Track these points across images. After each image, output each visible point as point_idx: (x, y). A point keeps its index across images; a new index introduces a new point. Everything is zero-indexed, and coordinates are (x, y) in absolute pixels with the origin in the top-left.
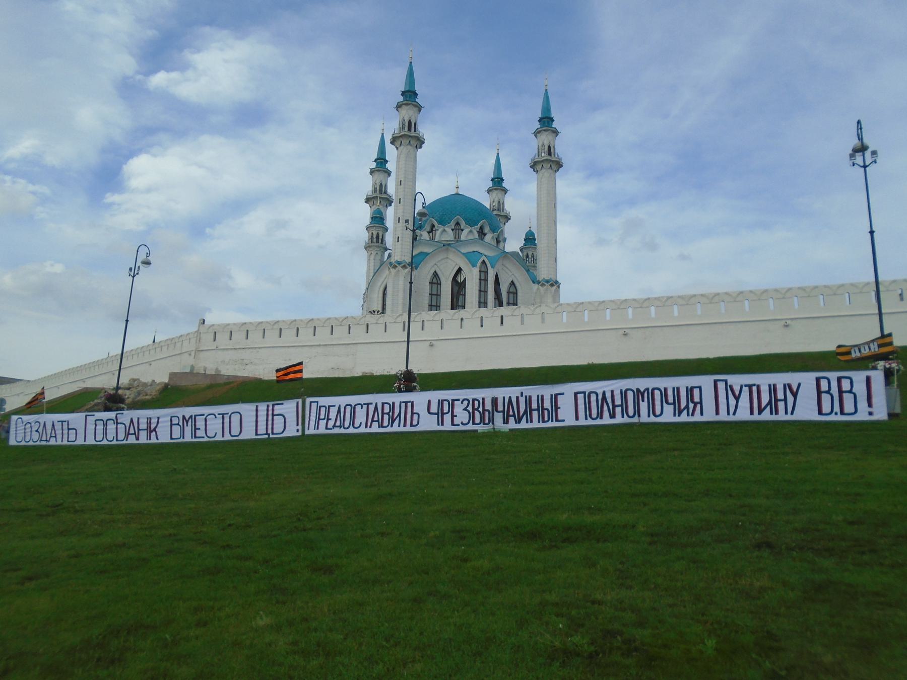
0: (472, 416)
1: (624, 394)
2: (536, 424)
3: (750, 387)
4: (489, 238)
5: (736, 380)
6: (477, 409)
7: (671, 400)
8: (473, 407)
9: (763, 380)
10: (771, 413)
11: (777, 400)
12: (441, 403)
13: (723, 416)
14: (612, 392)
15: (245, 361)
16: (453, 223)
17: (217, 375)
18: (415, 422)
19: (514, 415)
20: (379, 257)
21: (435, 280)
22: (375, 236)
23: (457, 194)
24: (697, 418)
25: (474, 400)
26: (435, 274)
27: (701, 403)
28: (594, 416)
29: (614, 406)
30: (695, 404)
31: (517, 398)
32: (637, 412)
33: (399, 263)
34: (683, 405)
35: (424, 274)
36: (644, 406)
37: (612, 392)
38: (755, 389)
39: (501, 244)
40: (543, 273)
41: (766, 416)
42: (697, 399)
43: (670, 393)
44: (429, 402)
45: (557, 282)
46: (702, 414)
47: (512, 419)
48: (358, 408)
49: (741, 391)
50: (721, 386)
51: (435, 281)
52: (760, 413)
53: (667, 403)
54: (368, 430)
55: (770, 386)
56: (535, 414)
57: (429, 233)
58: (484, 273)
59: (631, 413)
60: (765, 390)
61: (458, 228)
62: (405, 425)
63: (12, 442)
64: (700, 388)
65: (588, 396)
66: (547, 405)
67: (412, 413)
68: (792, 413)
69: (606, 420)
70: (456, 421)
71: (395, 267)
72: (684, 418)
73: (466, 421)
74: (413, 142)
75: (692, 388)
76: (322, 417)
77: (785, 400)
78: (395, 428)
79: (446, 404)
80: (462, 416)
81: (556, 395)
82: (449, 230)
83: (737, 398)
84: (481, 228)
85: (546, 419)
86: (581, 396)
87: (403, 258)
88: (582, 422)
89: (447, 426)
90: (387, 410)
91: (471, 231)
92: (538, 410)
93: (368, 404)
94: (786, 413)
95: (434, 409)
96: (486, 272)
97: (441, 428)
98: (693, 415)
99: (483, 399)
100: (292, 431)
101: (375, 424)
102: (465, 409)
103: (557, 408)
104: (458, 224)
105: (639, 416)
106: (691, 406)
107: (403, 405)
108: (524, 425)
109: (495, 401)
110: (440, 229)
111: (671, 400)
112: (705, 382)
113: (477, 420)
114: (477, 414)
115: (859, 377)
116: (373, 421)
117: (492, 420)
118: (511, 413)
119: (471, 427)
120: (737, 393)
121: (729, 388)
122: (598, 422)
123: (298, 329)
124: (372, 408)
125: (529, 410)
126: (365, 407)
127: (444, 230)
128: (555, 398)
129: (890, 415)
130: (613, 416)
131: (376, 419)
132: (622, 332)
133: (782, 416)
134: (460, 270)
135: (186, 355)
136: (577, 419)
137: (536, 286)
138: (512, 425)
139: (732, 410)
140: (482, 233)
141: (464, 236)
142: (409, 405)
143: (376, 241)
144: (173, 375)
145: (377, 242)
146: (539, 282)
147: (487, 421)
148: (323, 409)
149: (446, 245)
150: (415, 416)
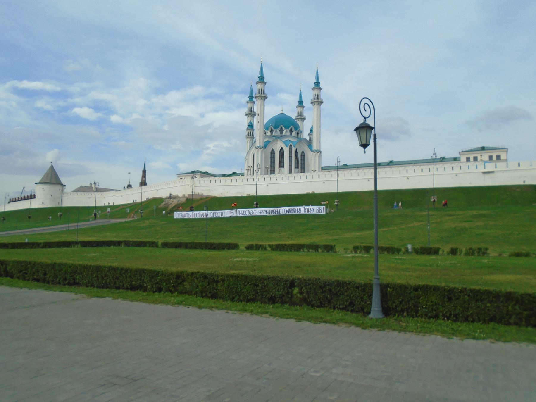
4: (294, 133)
16: (279, 128)
17: (202, 195)
21: (273, 152)
23: (282, 114)
39: (300, 135)
40: (315, 148)
45: (320, 151)
58: (291, 149)
61: (281, 131)
63: (175, 217)
74: (263, 98)
80: (265, 213)
84: (291, 129)
96: (292, 149)
100: (235, 215)
104: (282, 128)
110: (275, 130)
115: (322, 207)
129: (327, 213)
134: (282, 148)
135: (187, 186)
140: (291, 131)
141: (284, 133)
143: (251, 136)
149: (277, 138)
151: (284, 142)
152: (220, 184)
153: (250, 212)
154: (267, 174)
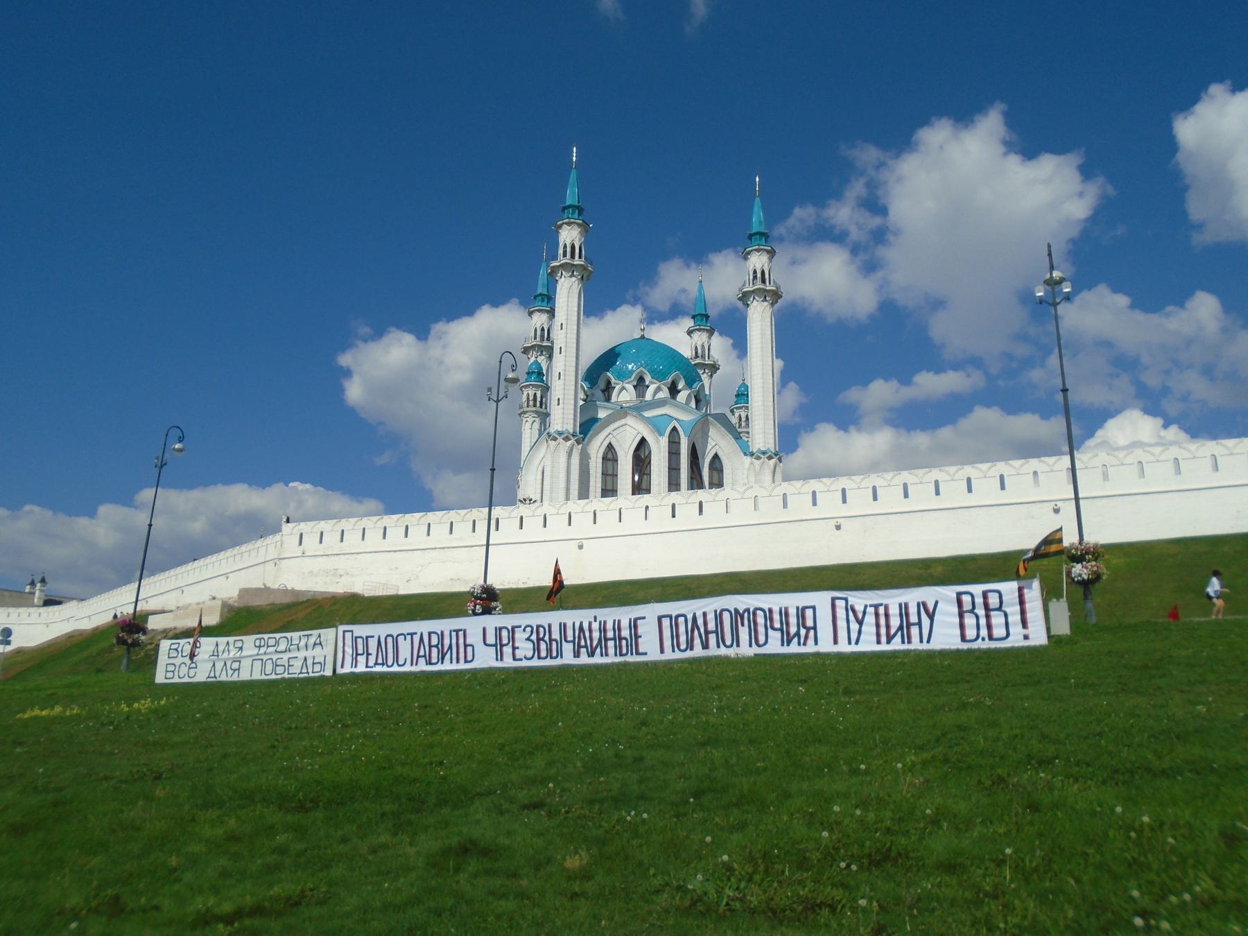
0: (537, 649)
1: (719, 617)
2: (611, 659)
3: (876, 607)
5: (859, 600)
6: (543, 639)
7: (777, 625)
8: (539, 637)
9: (893, 599)
10: (903, 642)
11: (909, 625)
12: (499, 630)
13: (844, 647)
14: (705, 614)
15: (340, 572)
18: (469, 658)
19: (586, 646)
20: (536, 426)
21: (610, 456)
24: (810, 648)
25: (538, 627)
26: (610, 447)
27: (815, 628)
28: (683, 646)
29: (707, 632)
30: (808, 629)
31: (590, 624)
32: (736, 640)
33: (560, 434)
34: (793, 630)
35: (596, 448)
36: (744, 633)
37: (705, 614)
38: (882, 610)
41: (897, 645)
42: (810, 623)
43: (776, 617)
44: (484, 629)
46: (816, 643)
47: (583, 650)
48: (401, 638)
49: (864, 613)
50: (840, 604)
51: (610, 456)
52: (888, 642)
53: (773, 628)
54: (414, 669)
55: (900, 605)
56: (611, 644)
57: (603, 391)
59: (728, 642)
60: (894, 610)
61: (640, 384)
62: (458, 661)
64: (814, 608)
65: (674, 620)
66: (625, 633)
67: (466, 646)
68: (928, 641)
69: (698, 652)
70: (519, 653)
71: (555, 439)
72: (794, 648)
73: (530, 654)
75: (804, 608)
76: (360, 651)
77: (919, 624)
78: (447, 666)
79: (505, 633)
80: (525, 648)
81: (636, 620)
82: (630, 387)
83: (860, 623)
85: (624, 651)
86: (666, 622)
87: (565, 427)
88: (669, 655)
89: (508, 662)
90: (435, 641)
91: (658, 389)
92: (614, 639)
93: (412, 634)
94: (921, 641)
95: (491, 639)
97: (499, 664)
98: (805, 644)
99: (550, 626)
101: (422, 661)
102: (528, 639)
103: (637, 637)
104: (641, 380)
105: (738, 645)
106: (803, 632)
107: (454, 634)
108: (598, 659)
109: (563, 627)
111: (777, 625)
112: (821, 600)
113: (543, 654)
114: (543, 646)
116: (418, 656)
117: (560, 653)
118: (583, 643)
119: (535, 663)
120: (860, 616)
121: (850, 609)
122: (688, 654)
123: (407, 527)
124: (417, 639)
125: (604, 639)
126: (409, 637)
127: (623, 388)
128: (634, 625)
130: (705, 646)
131: (422, 653)
132: (833, 522)
133: (916, 645)
134: (643, 441)
136: (662, 651)
137: (748, 460)
138: (584, 659)
139: (854, 636)
140: (674, 391)
142: (461, 633)
144: (244, 592)
146: (752, 454)
147: (554, 654)
148: (360, 641)
150: (469, 649)
151: (648, 421)
152: (385, 545)
153: (423, 648)
154: (584, 494)
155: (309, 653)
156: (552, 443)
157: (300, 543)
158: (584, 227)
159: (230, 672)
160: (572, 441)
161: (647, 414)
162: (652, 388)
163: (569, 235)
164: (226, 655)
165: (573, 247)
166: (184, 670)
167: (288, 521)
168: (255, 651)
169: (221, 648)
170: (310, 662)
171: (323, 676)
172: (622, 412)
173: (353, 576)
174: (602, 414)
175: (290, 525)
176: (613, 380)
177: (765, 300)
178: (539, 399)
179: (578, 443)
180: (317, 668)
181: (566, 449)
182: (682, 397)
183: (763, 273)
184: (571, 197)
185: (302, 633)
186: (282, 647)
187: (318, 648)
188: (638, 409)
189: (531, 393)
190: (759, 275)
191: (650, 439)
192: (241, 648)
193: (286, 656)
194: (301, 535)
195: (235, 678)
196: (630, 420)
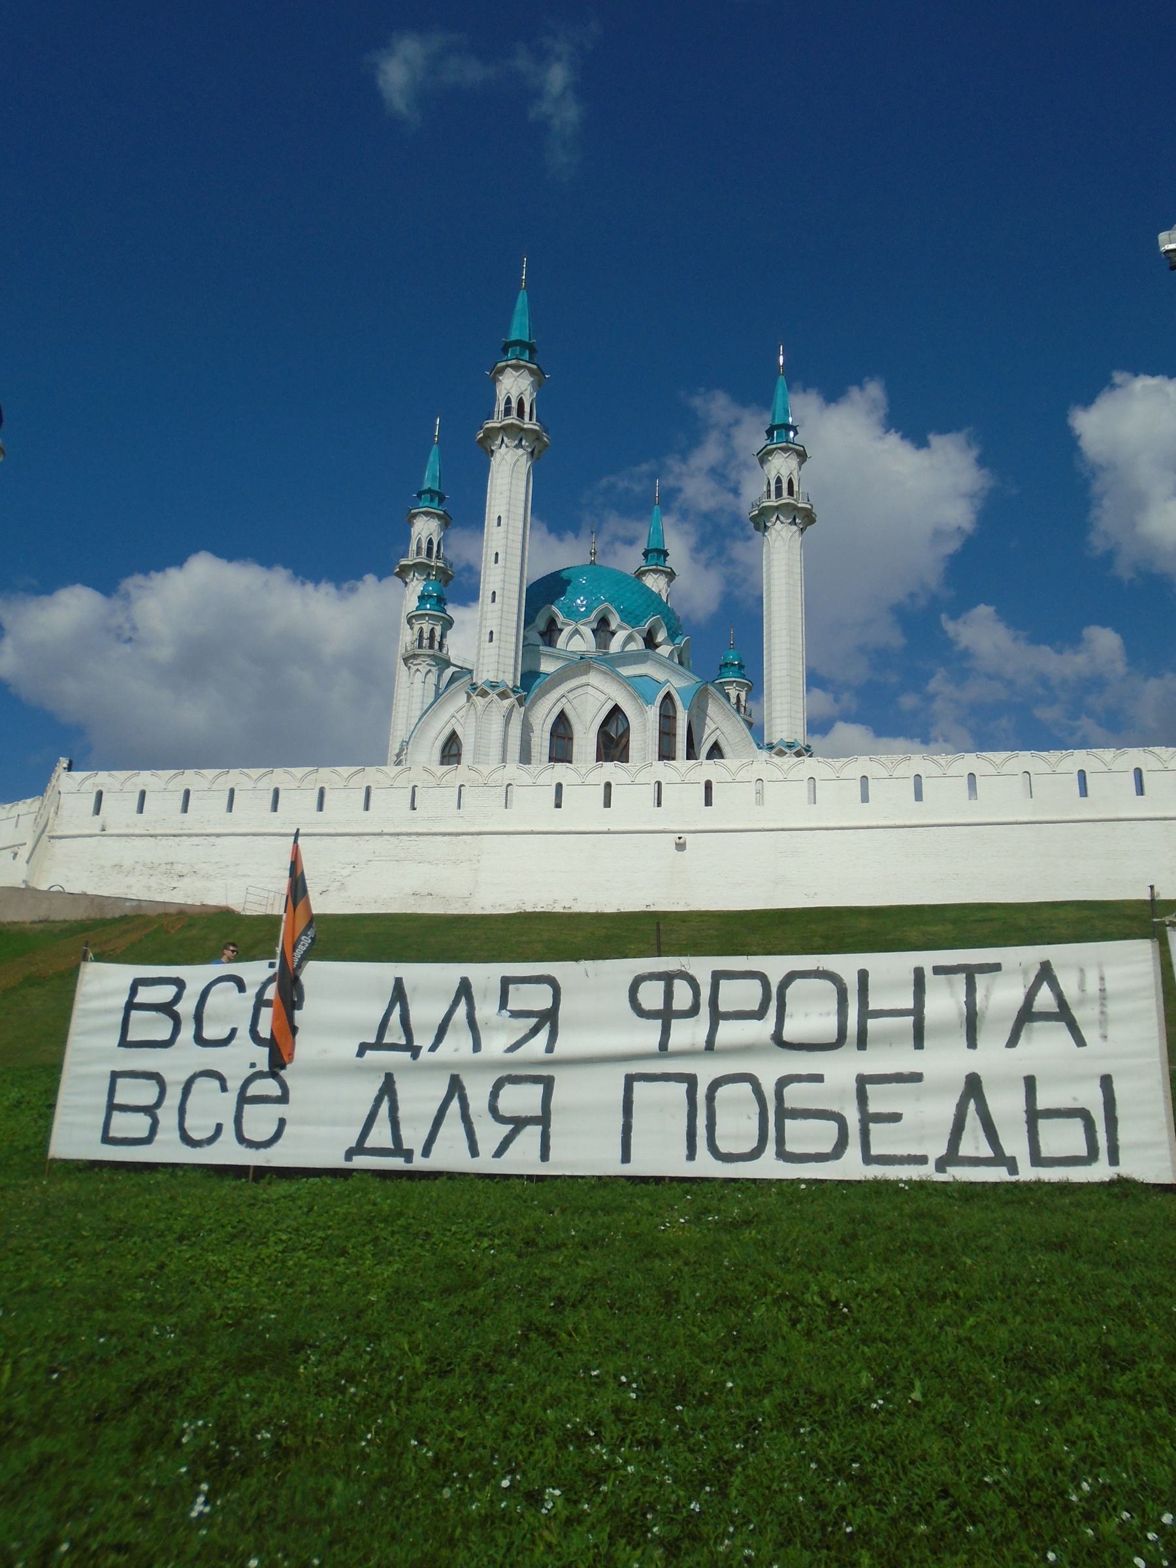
15: (178, 868)
20: (432, 678)
21: (562, 729)
22: (426, 635)
26: (562, 720)
33: (494, 686)
51: (561, 730)
57: (542, 634)
61: (603, 629)
71: (484, 694)
82: (587, 631)
91: (630, 639)
104: (604, 622)
127: (576, 632)
134: (616, 710)
135: (8, 854)
137: (764, 754)
140: (650, 642)
141: (615, 645)
145: (431, 647)
146: (771, 747)
151: (628, 683)
155: (992, 1058)
156: (479, 701)
157: (97, 810)
158: (538, 375)
159: (490, 1133)
160: (512, 700)
161: (627, 671)
162: (621, 636)
163: (514, 385)
164: (457, 1046)
165: (521, 403)
166: (210, 1107)
167: (70, 768)
168: (647, 1036)
169: (426, 1012)
170: (1007, 1105)
171: (1123, 1188)
172: (580, 665)
173: (207, 877)
174: (547, 666)
175: (78, 775)
176: (561, 618)
177: (794, 522)
178: (438, 638)
179: (521, 705)
180: (1064, 1138)
181: (504, 711)
182: (664, 650)
183: (790, 483)
184: (519, 329)
185: (928, 959)
186: (812, 1016)
187: (1046, 1045)
188: (610, 663)
189: (427, 628)
190: (785, 486)
191: (628, 708)
192: (549, 1018)
193: (841, 1070)
194: (100, 795)
195: (523, 1158)
196: (594, 678)
